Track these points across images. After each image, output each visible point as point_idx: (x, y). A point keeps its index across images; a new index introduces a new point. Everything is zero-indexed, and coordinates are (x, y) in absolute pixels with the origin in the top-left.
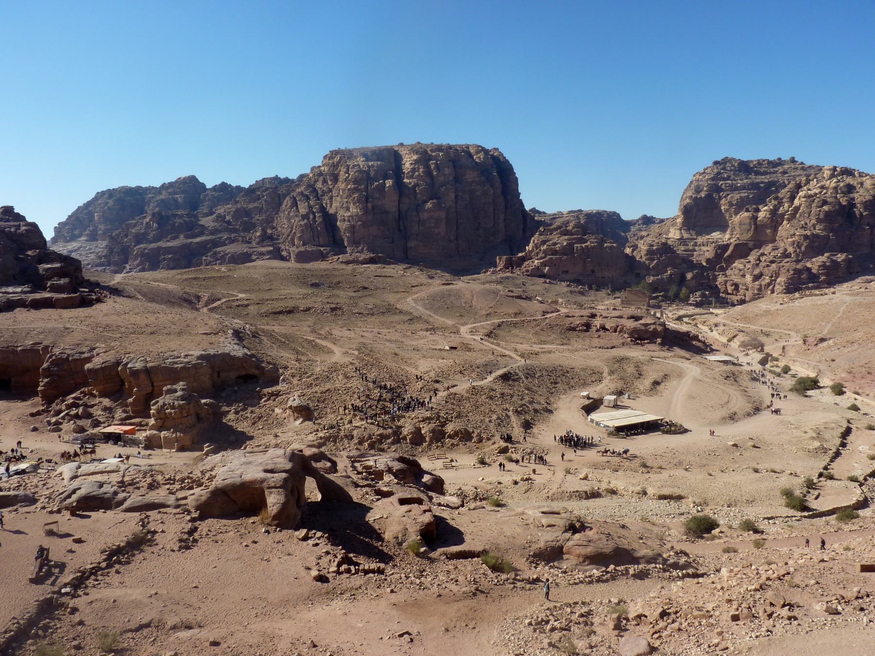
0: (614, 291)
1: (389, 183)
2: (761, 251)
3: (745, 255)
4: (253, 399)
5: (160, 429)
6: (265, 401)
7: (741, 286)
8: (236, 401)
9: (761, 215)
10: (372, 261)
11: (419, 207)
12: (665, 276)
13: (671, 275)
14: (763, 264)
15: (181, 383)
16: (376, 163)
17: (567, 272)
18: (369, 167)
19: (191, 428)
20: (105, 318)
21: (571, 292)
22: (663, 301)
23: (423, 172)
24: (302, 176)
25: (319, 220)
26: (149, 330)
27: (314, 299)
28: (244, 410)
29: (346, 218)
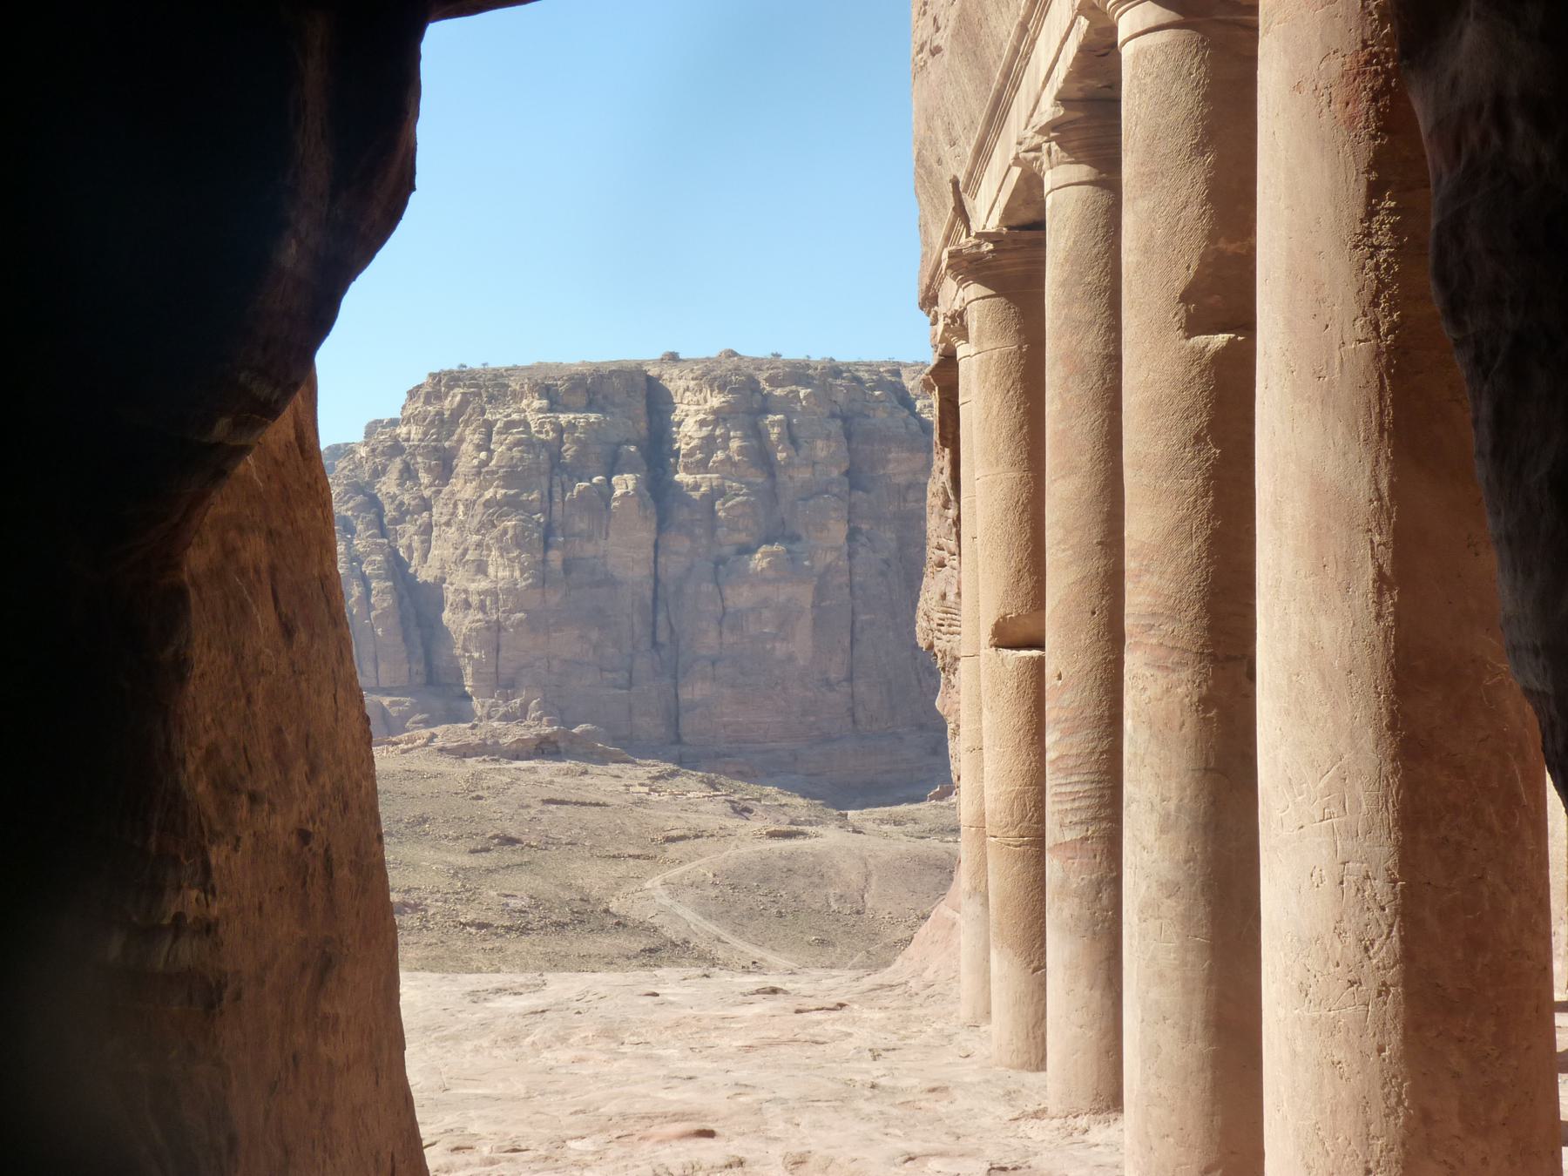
1: (624, 483)
10: (544, 749)
11: (723, 568)
16: (581, 419)
18: (560, 430)
23: (741, 451)
29: (474, 600)
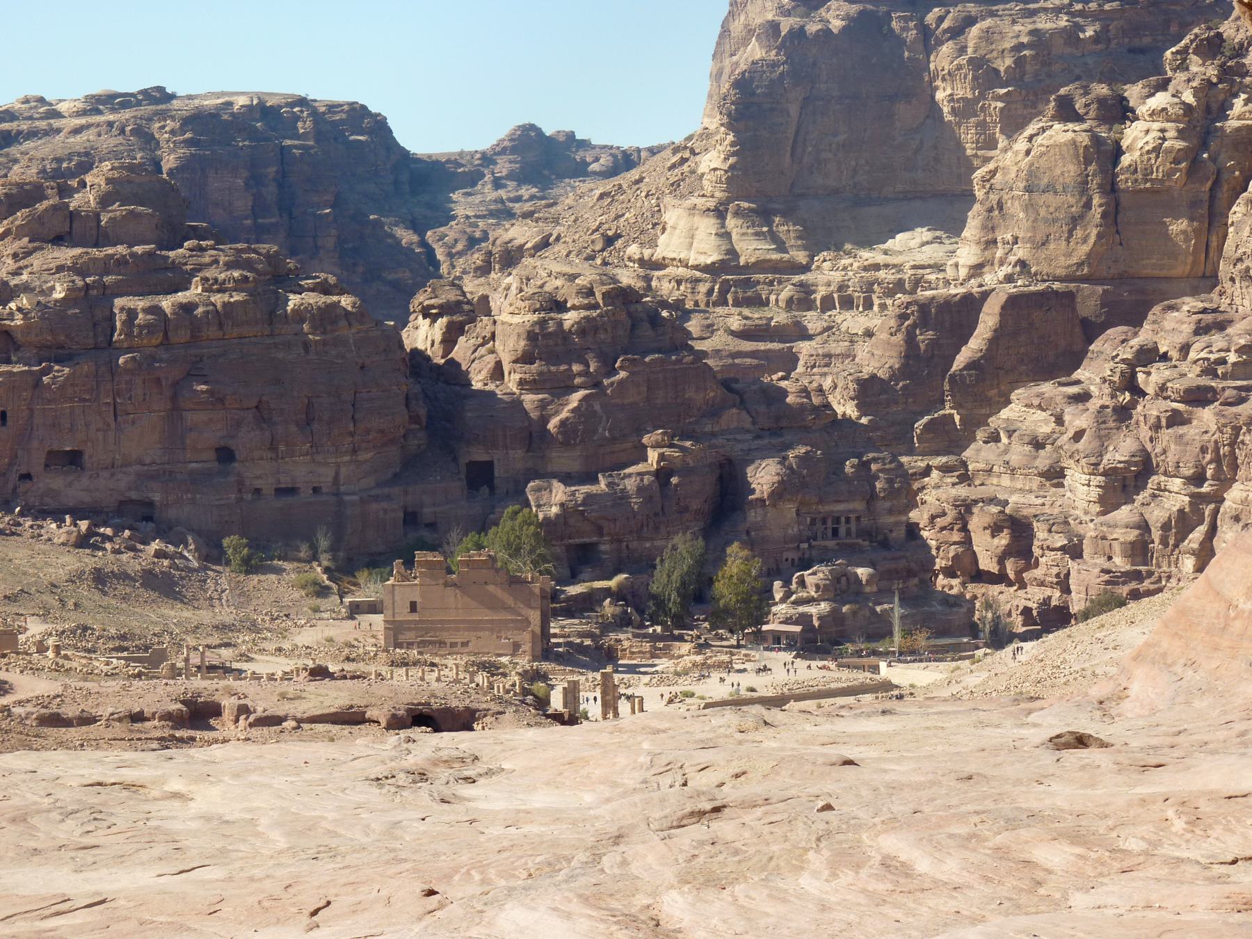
0: (346, 569)
2: (1144, 336)
3: (1060, 361)
7: (1040, 533)
9: (1137, 138)
12: (633, 478)
13: (662, 475)
14: (1151, 409)
17: (74, 459)
21: (100, 579)
22: (623, 622)
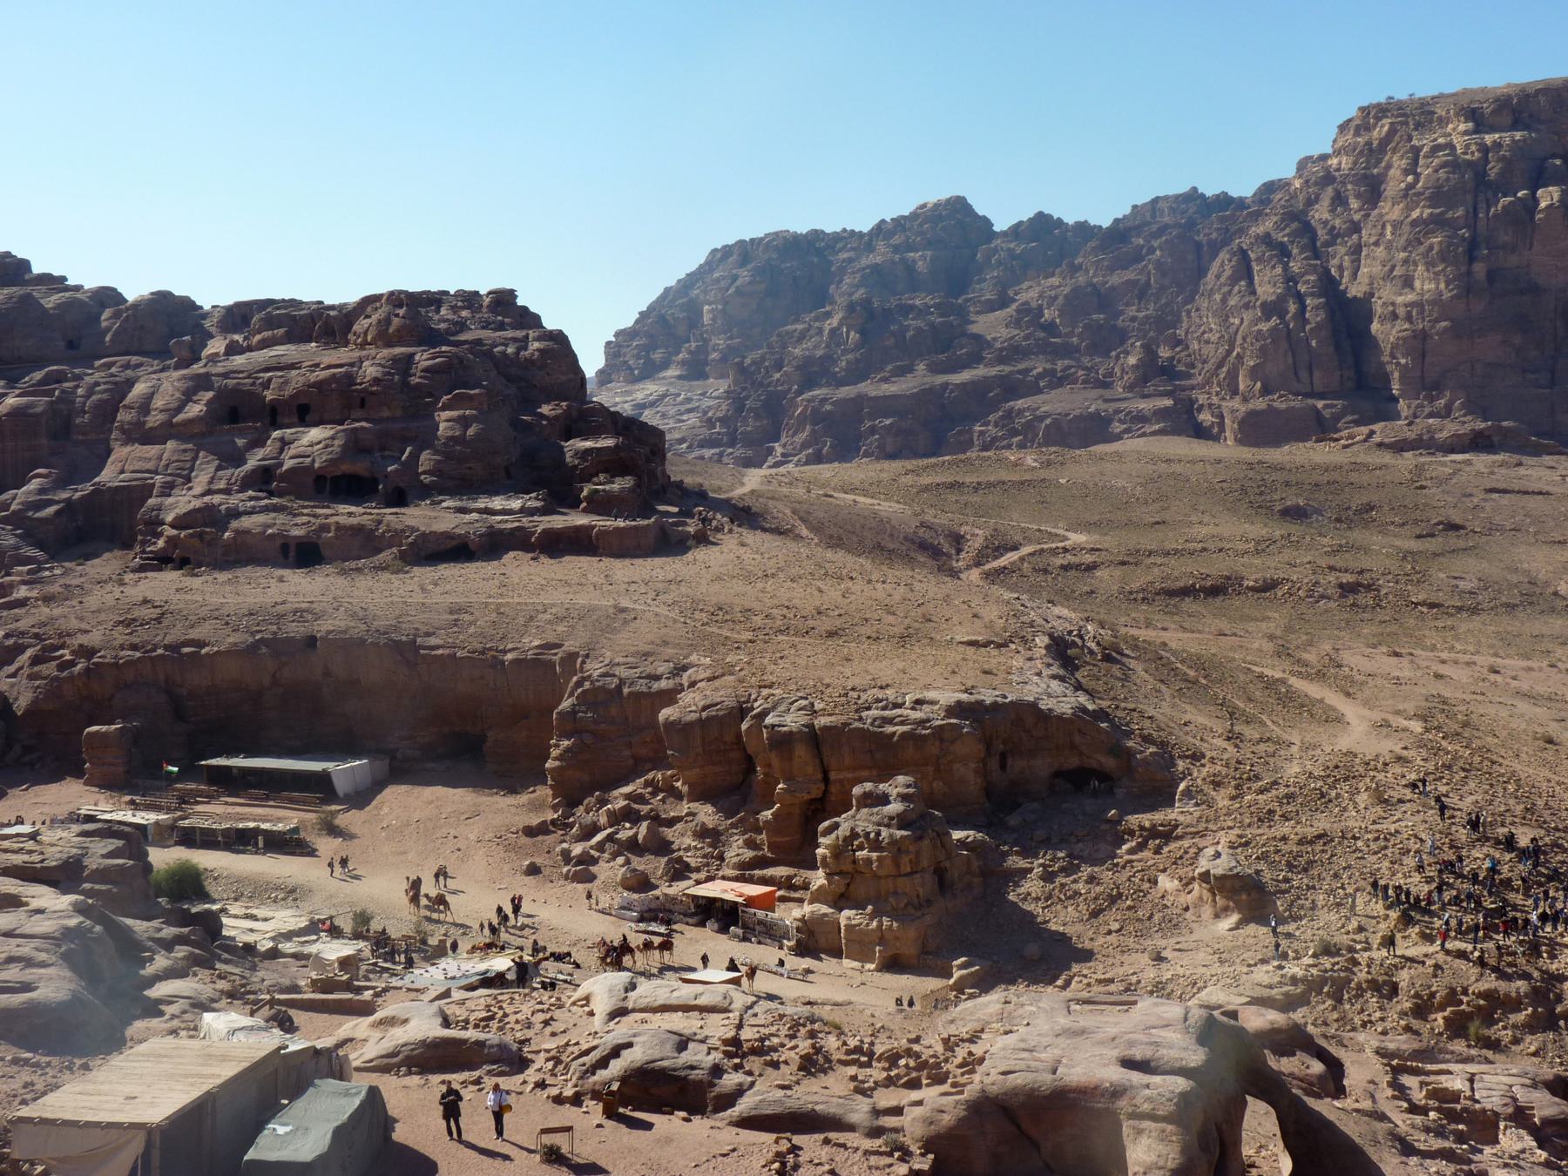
4: (1098, 842)
5: (841, 900)
6: (1131, 851)
8: (1047, 843)
10: (1478, 443)
15: (901, 779)
16: (1506, 138)
18: (1484, 149)
19: (920, 907)
20: (716, 587)
24: (1269, 188)
25: (1315, 317)
26: (825, 625)
27: (1288, 555)
28: (1069, 870)
29: (1401, 311)
